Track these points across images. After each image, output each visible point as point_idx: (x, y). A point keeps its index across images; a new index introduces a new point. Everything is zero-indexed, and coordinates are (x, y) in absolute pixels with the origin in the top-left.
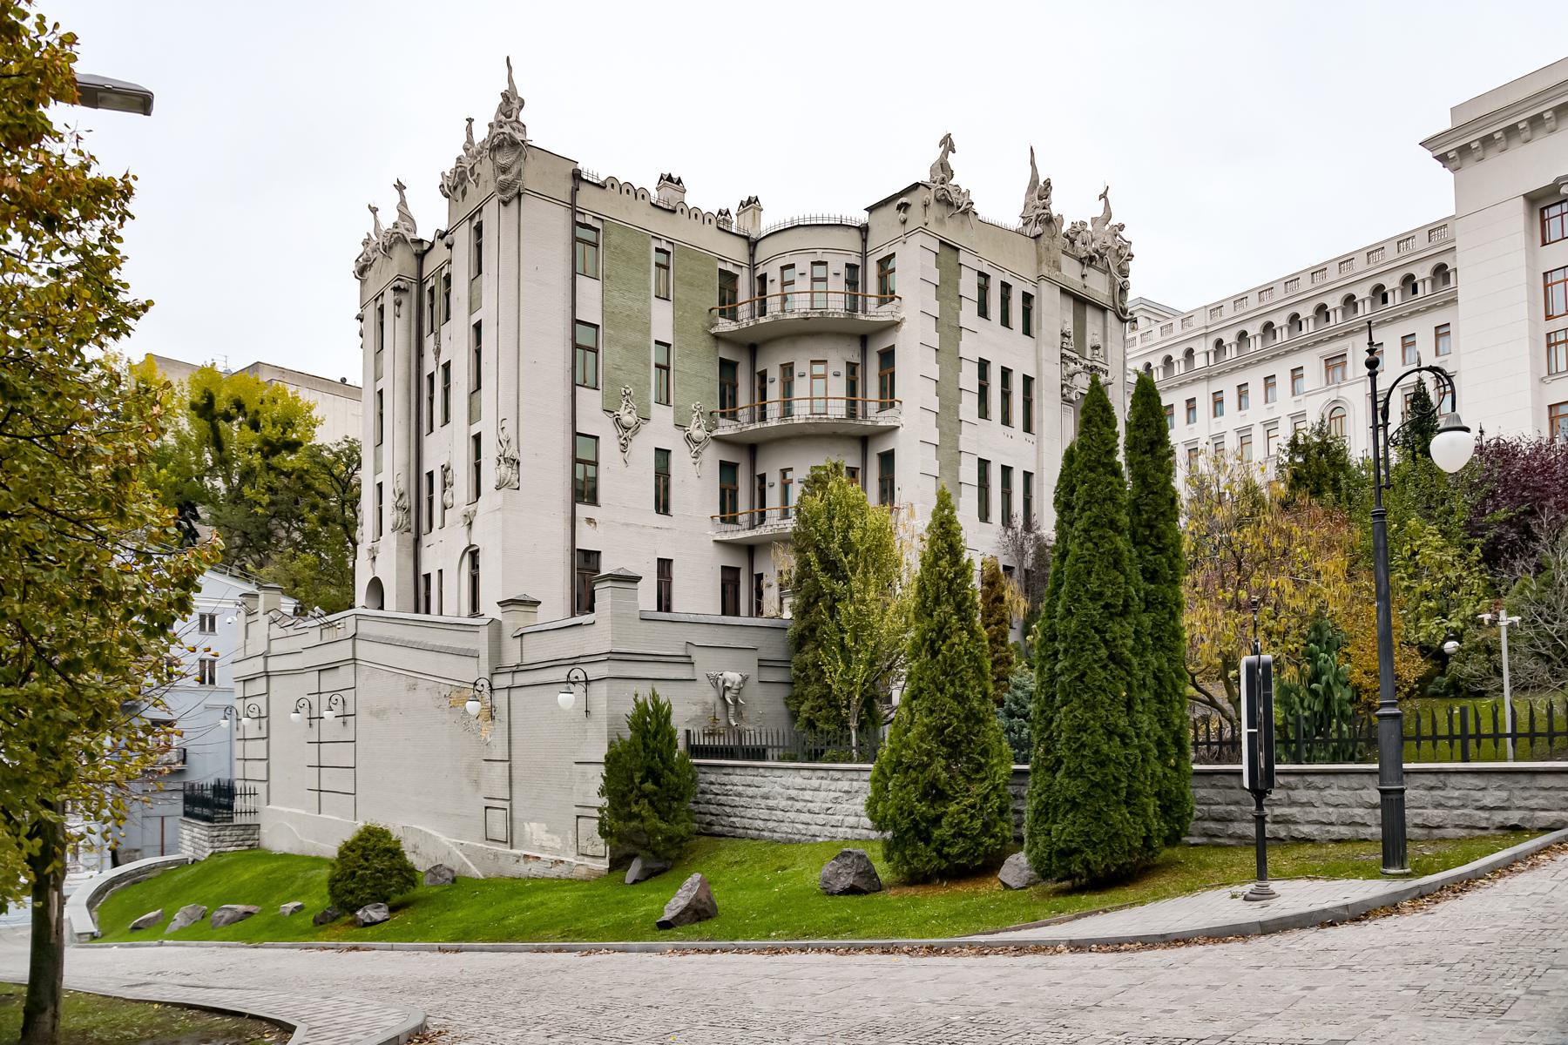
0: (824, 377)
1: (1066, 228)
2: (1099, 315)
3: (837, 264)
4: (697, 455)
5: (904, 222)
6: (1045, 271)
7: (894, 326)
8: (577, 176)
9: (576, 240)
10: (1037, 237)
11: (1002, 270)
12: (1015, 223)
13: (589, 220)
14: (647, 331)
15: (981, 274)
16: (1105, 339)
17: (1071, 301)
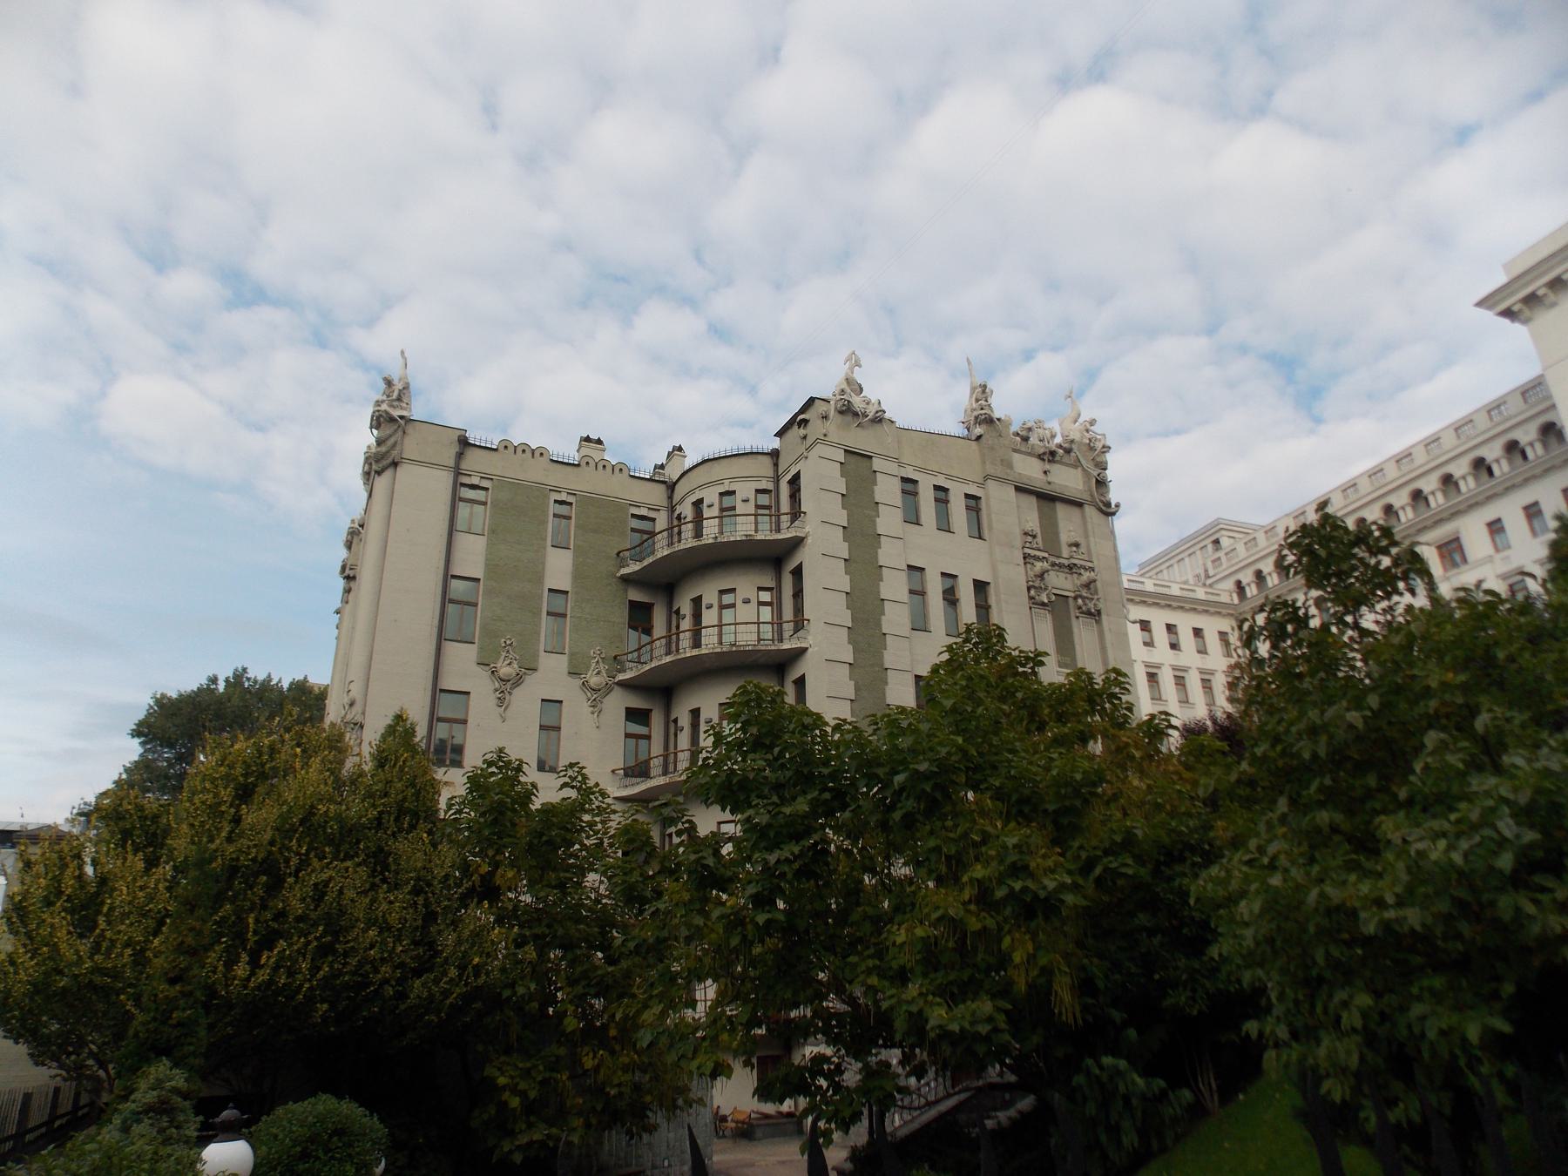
0: (733, 606)
1: (1014, 428)
2: (1075, 511)
3: (745, 490)
4: (594, 704)
5: (805, 437)
6: (990, 470)
7: (797, 543)
8: (464, 443)
9: (456, 499)
10: (979, 438)
11: (934, 473)
12: (960, 430)
13: (475, 481)
14: (540, 579)
15: (905, 480)
16: (1087, 537)
17: (1033, 499)
